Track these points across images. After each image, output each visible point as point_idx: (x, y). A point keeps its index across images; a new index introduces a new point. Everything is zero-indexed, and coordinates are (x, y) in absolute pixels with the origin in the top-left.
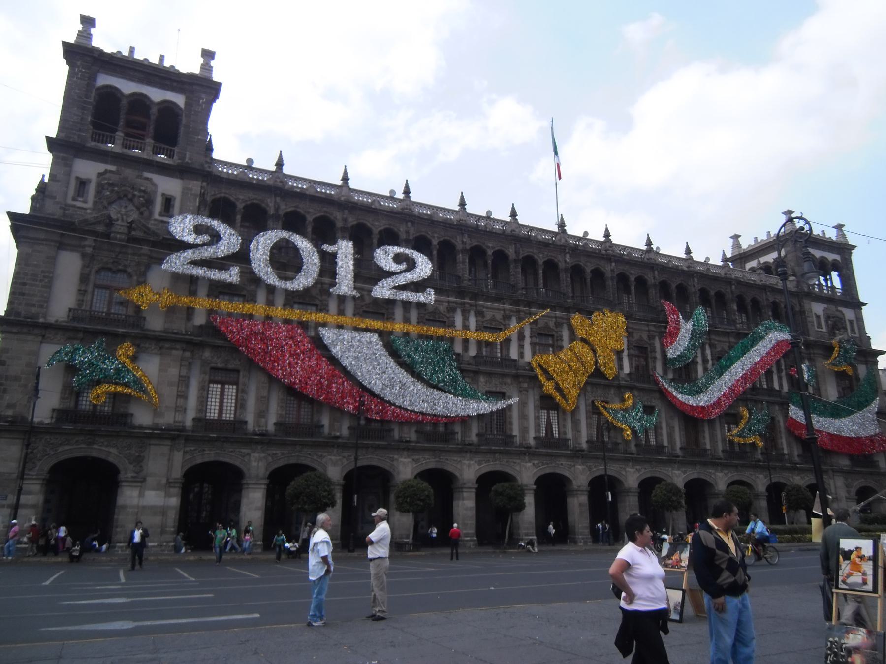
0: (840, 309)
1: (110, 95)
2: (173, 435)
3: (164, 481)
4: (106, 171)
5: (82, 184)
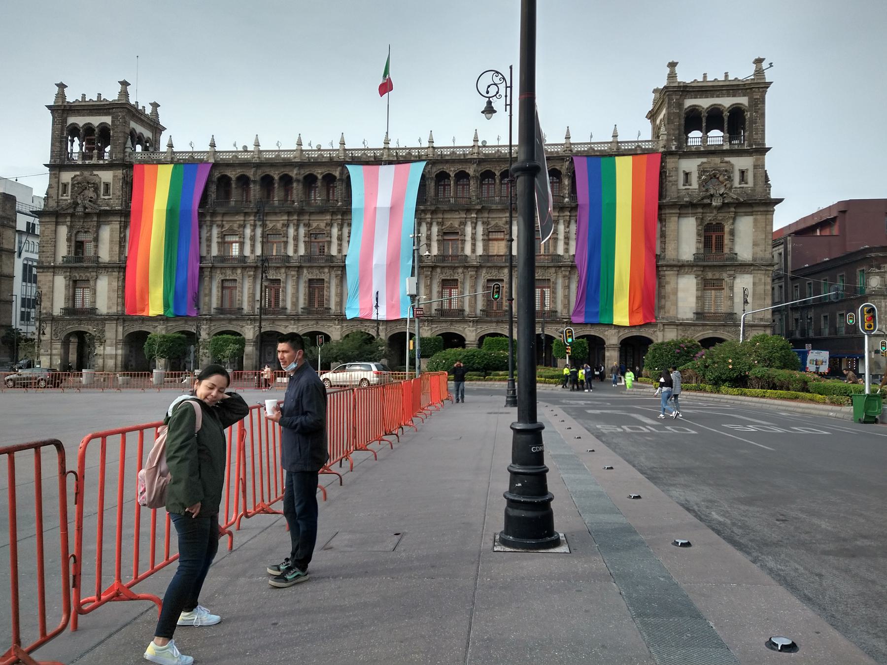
0: (727, 159)
4: (75, 176)
5: (65, 186)
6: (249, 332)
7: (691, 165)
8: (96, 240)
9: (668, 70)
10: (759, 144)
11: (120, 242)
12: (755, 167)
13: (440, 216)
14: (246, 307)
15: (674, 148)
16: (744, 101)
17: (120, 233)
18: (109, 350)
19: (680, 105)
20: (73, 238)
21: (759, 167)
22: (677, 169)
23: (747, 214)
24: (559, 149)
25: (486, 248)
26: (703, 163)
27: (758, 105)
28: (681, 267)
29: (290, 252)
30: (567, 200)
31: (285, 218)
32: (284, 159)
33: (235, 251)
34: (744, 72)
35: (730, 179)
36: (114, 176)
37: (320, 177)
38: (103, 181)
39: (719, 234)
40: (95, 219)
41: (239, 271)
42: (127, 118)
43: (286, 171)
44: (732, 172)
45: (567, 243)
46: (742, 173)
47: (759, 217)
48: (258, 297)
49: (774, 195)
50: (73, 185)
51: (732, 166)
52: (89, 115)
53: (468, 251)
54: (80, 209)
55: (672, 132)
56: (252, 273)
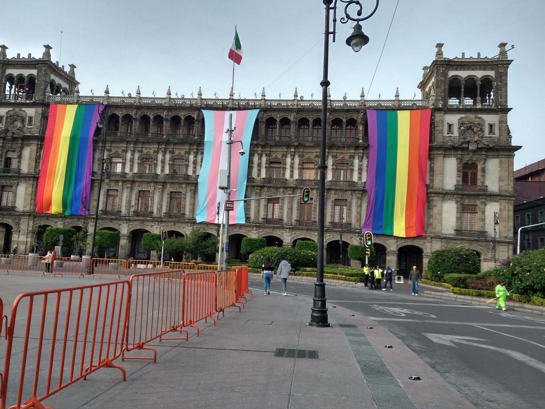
0: (479, 116)
3: (26, 232)
4: (9, 111)
6: (125, 229)
7: (453, 119)
8: (20, 157)
9: (436, 50)
10: (503, 106)
11: (36, 160)
12: (500, 122)
13: (268, 149)
14: (124, 211)
15: (440, 106)
16: (492, 73)
17: (37, 152)
18: (22, 238)
19: (445, 75)
20: (4, 155)
21: (503, 122)
22: (443, 122)
23: (494, 157)
24: (356, 104)
25: (300, 174)
26: (462, 118)
27: (502, 77)
28: (445, 195)
29: (159, 172)
30: (361, 141)
31: (156, 146)
32: (157, 104)
33: (119, 169)
34: (492, 53)
35: (482, 130)
36: (36, 112)
37: (183, 118)
38: (28, 115)
39: (473, 171)
40: (20, 142)
41: (120, 184)
42: (48, 72)
43: (159, 113)
44: (484, 125)
45: (360, 173)
46: (491, 126)
47: (503, 159)
48: (133, 203)
49: (514, 143)
50: (7, 117)
51: (483, 120)
52: (21, 68)
53: (287, 176)
54: (10, 134)
55: (439, 94)
56: (129, 185)
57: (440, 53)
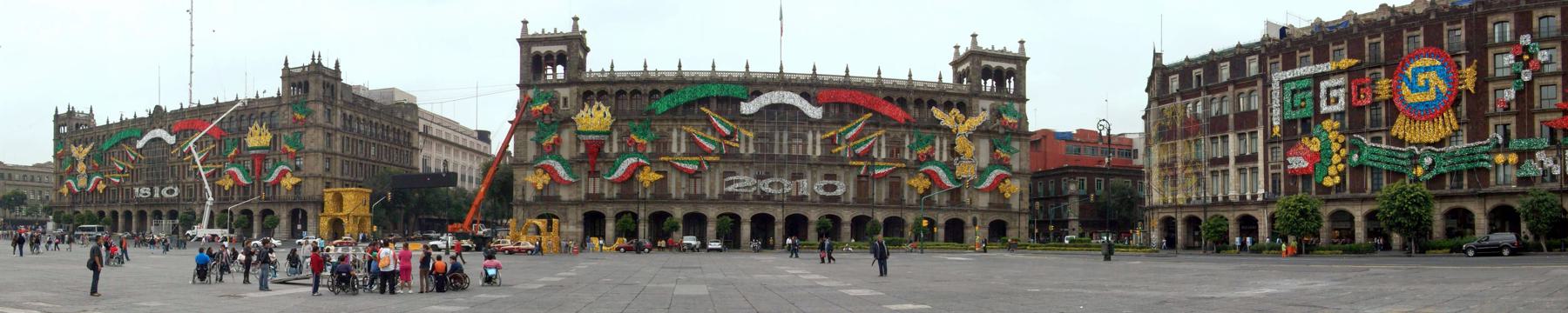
1: (537, 57)
2: (577, 203)
18: (572, 228)
21: (1023, 110)
27: (1022, 69)
34: (1014, 49)
57: (974, 42)
